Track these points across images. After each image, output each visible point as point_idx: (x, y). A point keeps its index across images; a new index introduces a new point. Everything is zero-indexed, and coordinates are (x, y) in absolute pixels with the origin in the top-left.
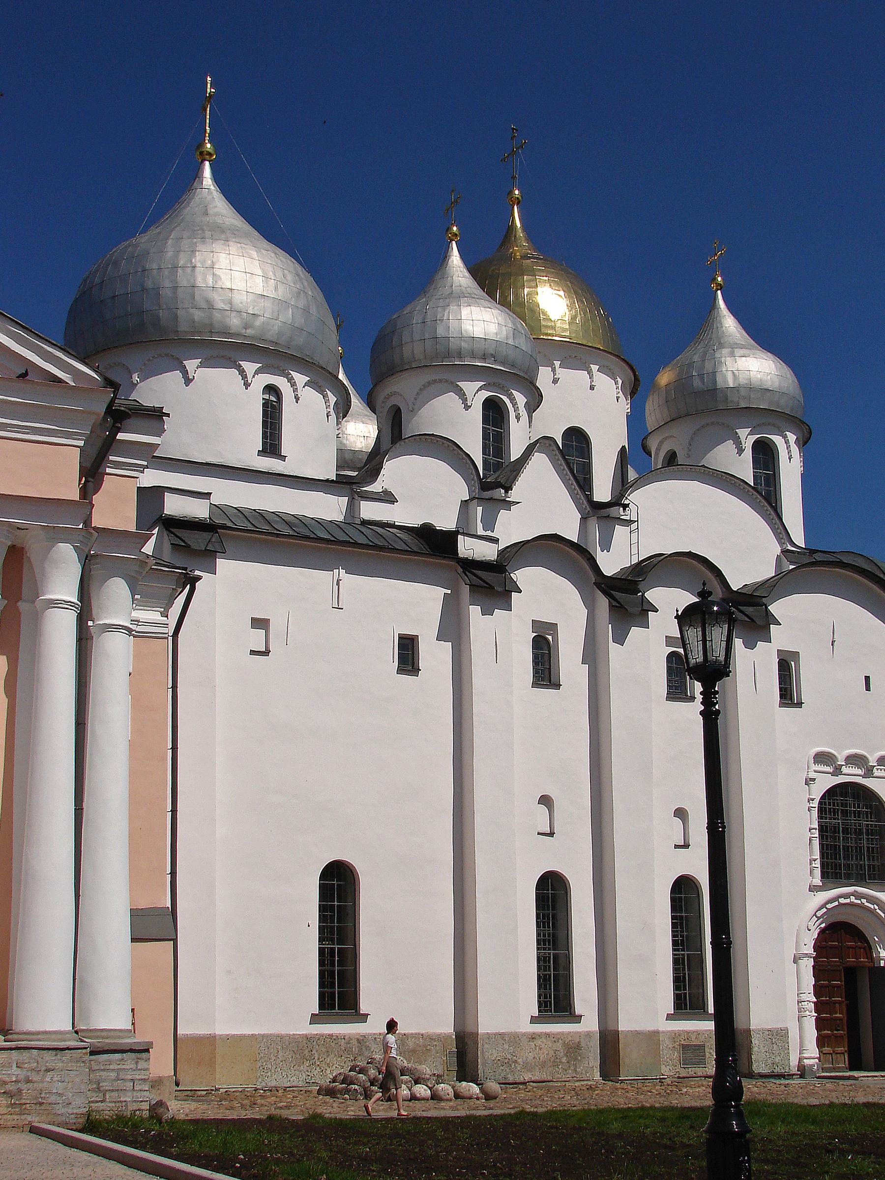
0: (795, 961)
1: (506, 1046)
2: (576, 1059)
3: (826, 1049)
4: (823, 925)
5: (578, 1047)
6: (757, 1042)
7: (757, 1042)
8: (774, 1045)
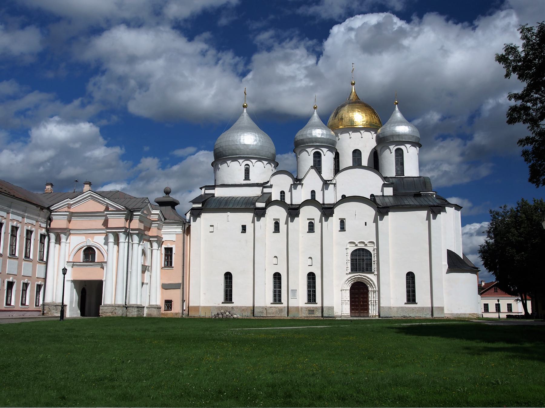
0: (341, 291)
1: (261, 309)
2: (281, 312)
3: (352, 312)
5: (282, 310)
6: (325, 309)
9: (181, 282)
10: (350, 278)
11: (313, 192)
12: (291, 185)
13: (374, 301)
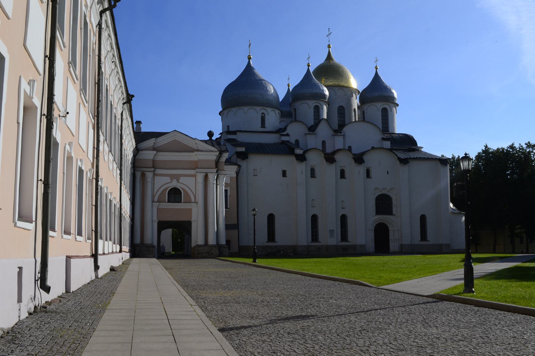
4: (377, 223)
9: (236, 223)
10: (376, 219)
11: (324, 143)
12: (306, 134)
13: (395, 240)
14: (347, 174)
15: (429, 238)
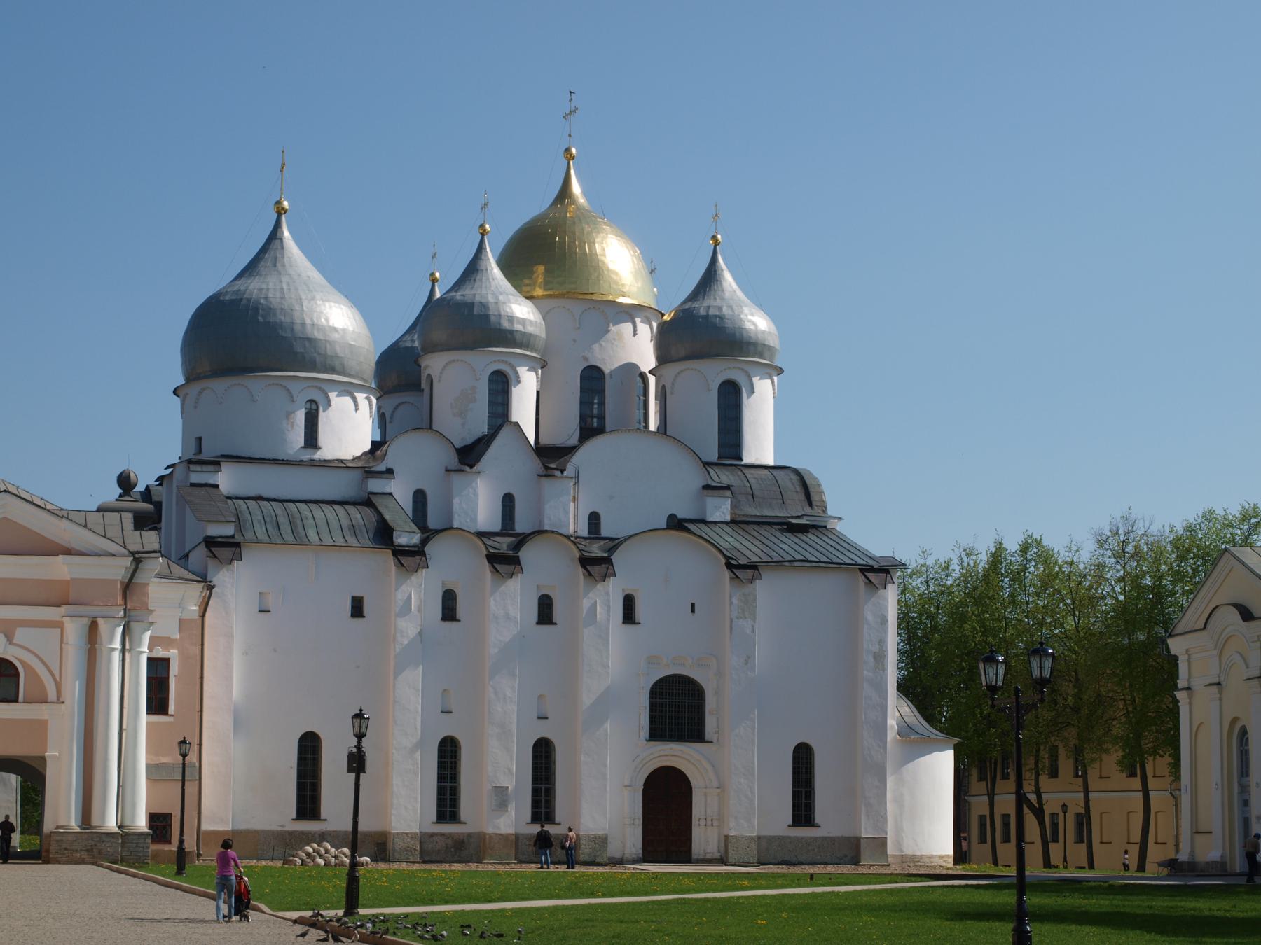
7: (584, 843)
8: (597, 845)
14: (558, 612)
15: (819, 817)
